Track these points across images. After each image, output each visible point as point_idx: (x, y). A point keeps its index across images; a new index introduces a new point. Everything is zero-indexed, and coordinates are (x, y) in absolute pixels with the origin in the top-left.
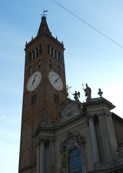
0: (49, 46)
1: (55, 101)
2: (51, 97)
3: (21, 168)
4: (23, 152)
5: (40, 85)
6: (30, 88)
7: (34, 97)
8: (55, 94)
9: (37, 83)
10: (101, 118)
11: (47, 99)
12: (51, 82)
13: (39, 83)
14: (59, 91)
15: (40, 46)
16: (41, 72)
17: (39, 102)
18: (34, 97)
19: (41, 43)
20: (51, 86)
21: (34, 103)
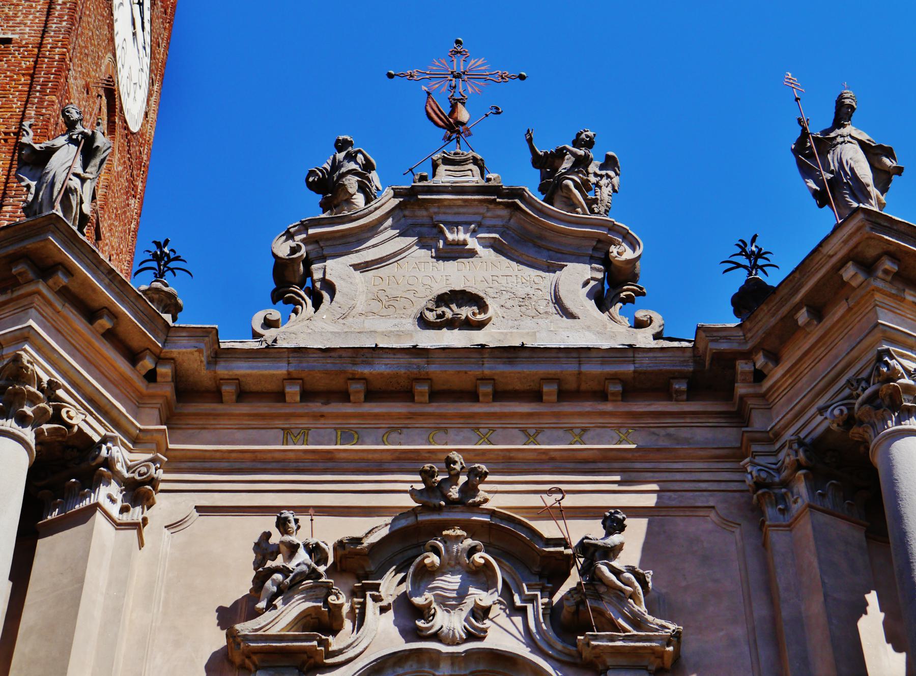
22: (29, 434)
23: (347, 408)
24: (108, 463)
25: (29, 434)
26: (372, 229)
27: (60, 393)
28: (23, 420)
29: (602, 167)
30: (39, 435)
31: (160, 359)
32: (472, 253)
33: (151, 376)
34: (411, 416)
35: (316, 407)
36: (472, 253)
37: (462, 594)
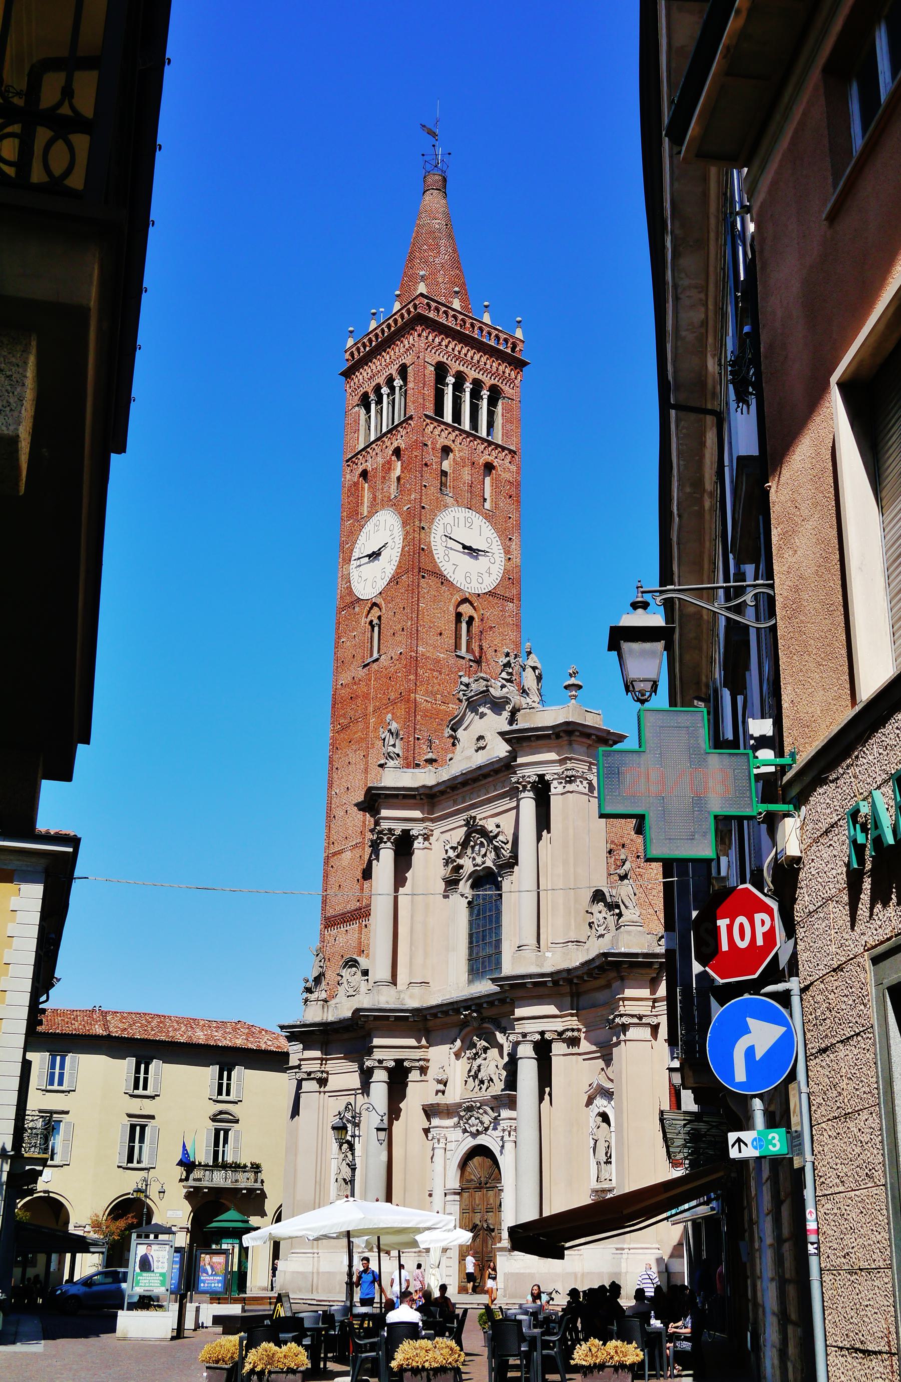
0: (441, 370)
1: (457, 646)
2: (441, 634)
3: (331, 912)
4: (334, 854)
5: (395, 580)
6: (363, 583)
7: (376, 629)
8: (459, 616)
9: (388, 564)
10: (560, 789)
11: (420, 649)
12: (440, 565)
13: (394, 568)
14: (479, 595)
15: (403, 371)
16: (401, 514)
17: (392, 658)
18: (376, 629)
19: (407, 360)
20: (443, 580)
21: (375, 655)
22: (389, 844)
23: (460, 791)
24: (413, 835)
25: (389, 844)
26: (464, 715)
27: (392, 827)
28: (385, 843)
29: (515, 659)
30: (391, 842)
31: (420, 795)
32: (486, 714)
33: (421, 799)
34: (473, 788)
35: (456, 792)
36: (486, 714)
37: (479, 851)
